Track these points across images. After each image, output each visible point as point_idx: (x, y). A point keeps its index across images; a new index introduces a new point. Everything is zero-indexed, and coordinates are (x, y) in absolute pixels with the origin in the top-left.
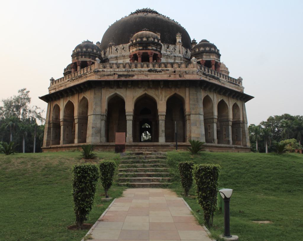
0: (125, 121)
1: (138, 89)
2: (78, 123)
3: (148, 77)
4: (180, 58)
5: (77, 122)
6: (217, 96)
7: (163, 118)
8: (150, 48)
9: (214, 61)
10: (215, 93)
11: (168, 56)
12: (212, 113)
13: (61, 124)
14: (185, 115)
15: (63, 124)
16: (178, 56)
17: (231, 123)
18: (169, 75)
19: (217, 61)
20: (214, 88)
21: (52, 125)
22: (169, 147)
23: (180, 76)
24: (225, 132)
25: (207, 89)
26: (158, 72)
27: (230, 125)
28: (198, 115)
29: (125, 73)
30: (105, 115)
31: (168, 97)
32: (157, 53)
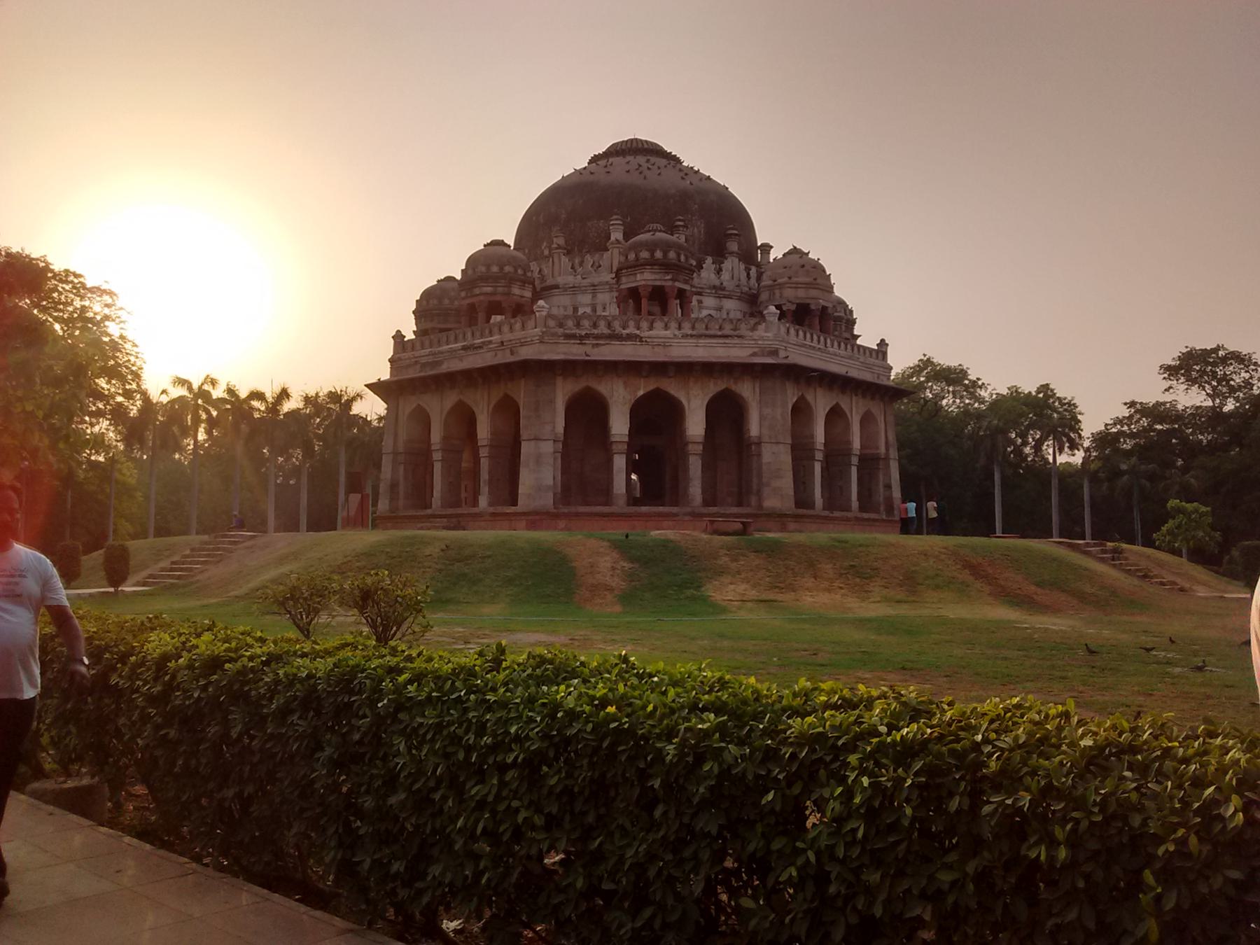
3: (462, 360)
4: (608, 287)
6: (625, 383)
8: (477, 291)
9: (644, 286)
11: (574, 287)
16: (601, 284)
18: (493, 353)
19: (658, 283)
22: (483, 518)
23: (512, 353)
26: (476, 348)
28: (533, 443)
29: (430, 359)
31: (493, 403)
32: (498, 298)
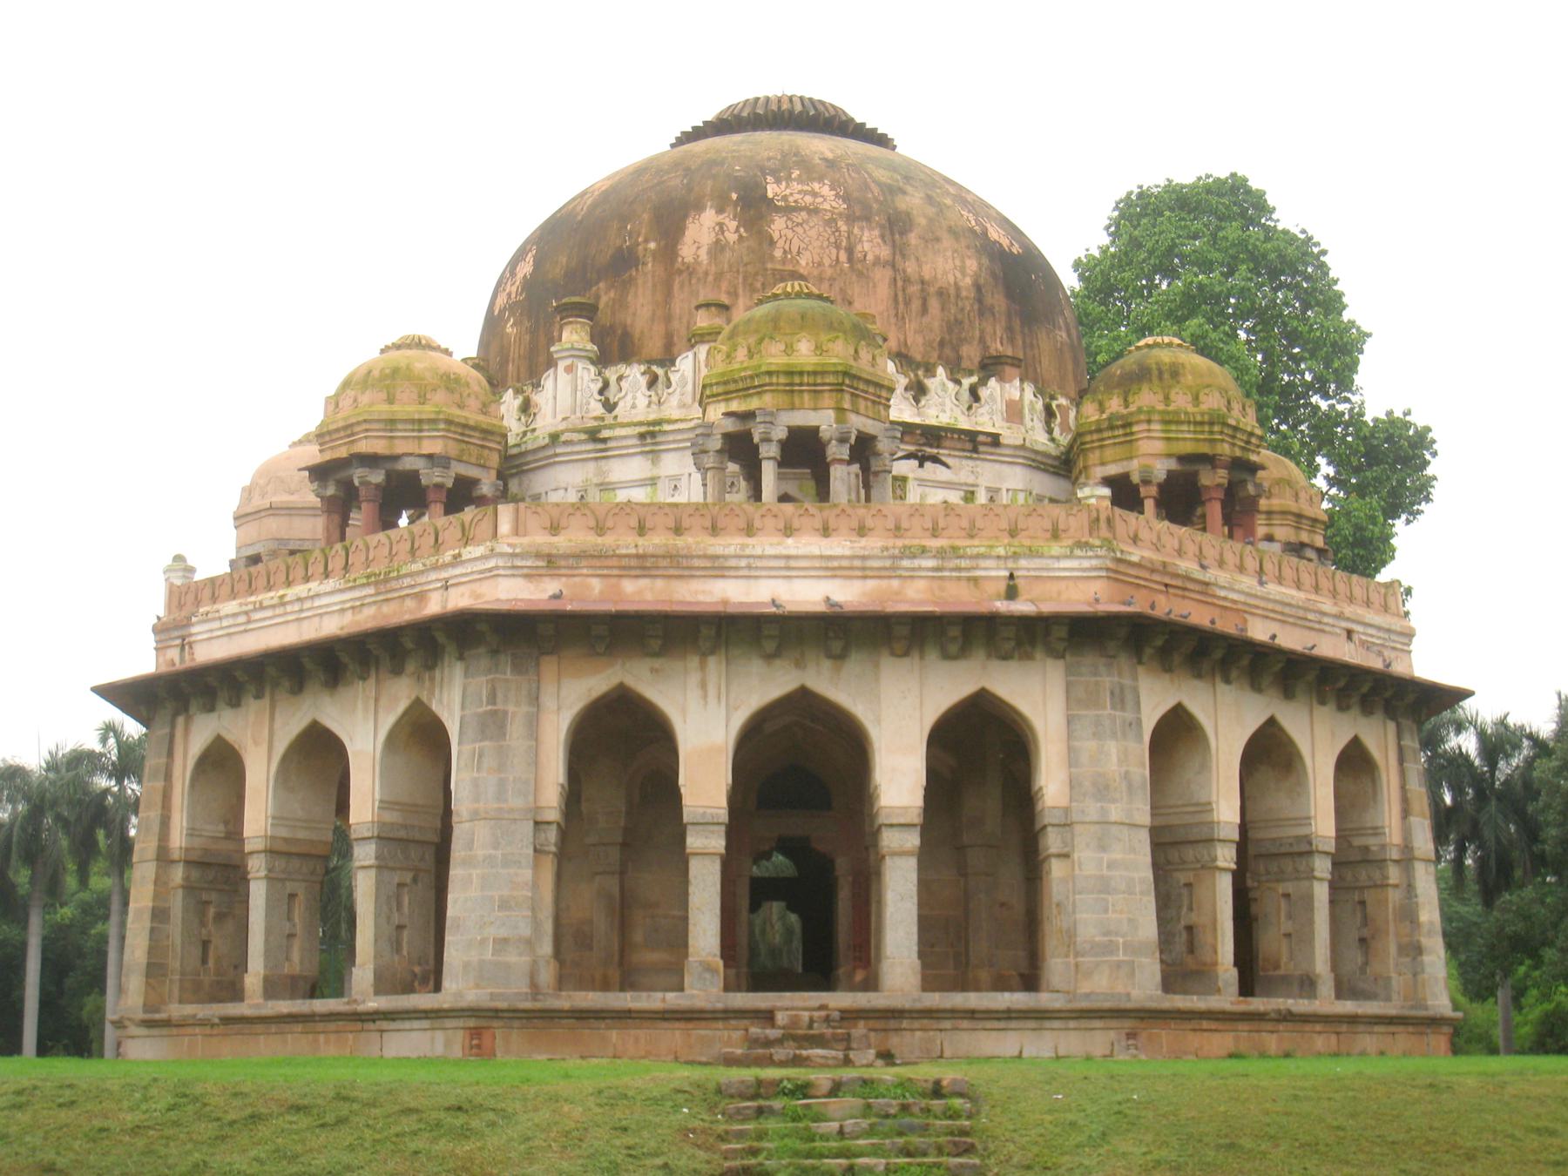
0: (679, 858)
1: (756, 666)
2: (381, 867)
5: (372, 862)
7: (913, 840)
10: (1227, 681)
12: (1207, 807)
13: (257, 867)
14: (1038, 826)
15: (263, 873)
17: (1322, 867)
20: (1218, 654)
21: (178, 874)
24: (1290, 917)
25: (1177, 659)
27: (1321, 879)
30: (558, 824)
